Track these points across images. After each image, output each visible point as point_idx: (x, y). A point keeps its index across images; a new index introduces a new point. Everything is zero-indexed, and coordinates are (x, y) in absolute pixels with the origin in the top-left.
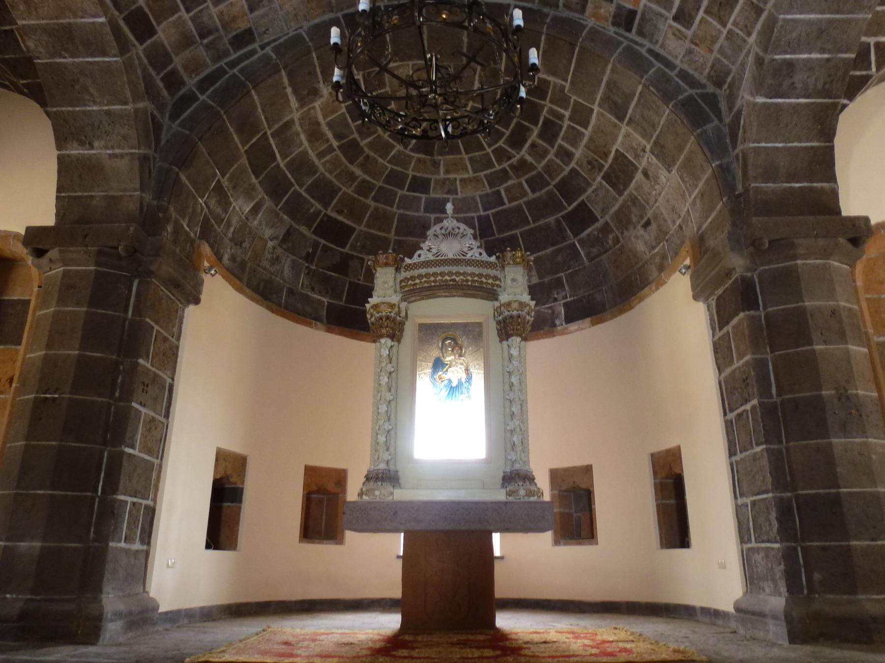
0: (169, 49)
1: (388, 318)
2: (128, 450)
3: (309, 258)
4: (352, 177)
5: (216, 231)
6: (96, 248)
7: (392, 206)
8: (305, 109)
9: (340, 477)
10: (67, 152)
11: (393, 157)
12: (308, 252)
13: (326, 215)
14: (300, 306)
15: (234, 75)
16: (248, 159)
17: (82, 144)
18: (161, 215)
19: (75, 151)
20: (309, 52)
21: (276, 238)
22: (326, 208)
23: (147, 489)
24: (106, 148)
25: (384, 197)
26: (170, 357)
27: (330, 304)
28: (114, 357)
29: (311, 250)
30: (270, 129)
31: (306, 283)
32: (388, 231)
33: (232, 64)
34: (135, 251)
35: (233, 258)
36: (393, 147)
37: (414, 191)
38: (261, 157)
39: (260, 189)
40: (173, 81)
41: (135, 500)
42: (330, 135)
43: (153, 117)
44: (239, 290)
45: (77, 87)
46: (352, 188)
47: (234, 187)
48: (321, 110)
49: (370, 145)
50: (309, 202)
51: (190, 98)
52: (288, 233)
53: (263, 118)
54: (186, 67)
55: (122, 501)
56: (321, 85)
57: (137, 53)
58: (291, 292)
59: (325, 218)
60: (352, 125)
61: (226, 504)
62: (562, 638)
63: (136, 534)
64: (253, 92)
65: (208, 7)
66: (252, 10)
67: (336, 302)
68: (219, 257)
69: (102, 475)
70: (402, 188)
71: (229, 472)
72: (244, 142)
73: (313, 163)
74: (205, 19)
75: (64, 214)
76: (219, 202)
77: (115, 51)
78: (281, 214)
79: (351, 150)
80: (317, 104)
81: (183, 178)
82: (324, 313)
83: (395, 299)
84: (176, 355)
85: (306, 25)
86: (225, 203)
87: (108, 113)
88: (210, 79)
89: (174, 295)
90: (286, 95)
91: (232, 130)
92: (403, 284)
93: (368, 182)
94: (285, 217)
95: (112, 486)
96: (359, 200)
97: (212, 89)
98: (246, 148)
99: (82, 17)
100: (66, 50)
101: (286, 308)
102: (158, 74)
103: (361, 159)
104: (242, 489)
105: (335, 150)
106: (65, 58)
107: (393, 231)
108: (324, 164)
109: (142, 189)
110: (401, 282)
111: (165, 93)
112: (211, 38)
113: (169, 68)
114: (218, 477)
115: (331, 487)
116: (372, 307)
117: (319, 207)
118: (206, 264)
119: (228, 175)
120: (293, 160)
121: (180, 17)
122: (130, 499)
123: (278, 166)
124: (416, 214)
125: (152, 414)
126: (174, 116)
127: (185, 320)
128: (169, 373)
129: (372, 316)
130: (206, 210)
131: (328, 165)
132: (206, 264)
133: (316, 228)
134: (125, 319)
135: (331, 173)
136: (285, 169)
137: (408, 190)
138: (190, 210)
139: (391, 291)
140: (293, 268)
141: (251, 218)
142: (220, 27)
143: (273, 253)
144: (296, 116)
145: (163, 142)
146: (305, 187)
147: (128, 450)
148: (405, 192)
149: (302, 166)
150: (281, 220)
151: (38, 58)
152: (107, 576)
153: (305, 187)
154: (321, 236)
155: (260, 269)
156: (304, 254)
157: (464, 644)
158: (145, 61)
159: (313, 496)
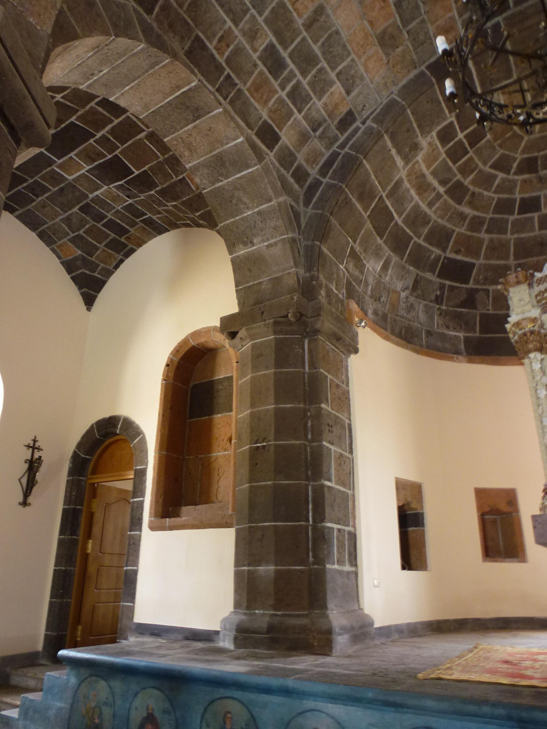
0: (292, 148)
1: (532, 332)
2: (327, 483)
3: (438, 300)
4: (462, 217)
5: (357, 291)
6: (272, 320)
7: (506, 233)
8: (410, 166)
9: (510, 497)
10: (237, 254)
11: (498, 186)
12: (437, 296)
13: (445, 258)
14: (439, 344)
15: (347, 153)
16: (371, 223)
17: (245, 244)
18: (314, 283)
19: (242, 251)
20: (404, 110)
21: (407, 288)
22: (444, 252)
23: (346, 516)
24: (264, 242)
25: (497, 227)
26: (344, 401)
27: (466, 338)
28: (302, 406)
29: (438, 293)
30: (384, 192)
31: (440, 322)
32: (507, 258)
33: (342, 146)
34: (302, 315)
35: (375, 313)
36: (496, 177)
37: (525, 213)
38: (381, 218)
39: (386, 248)
40: (300, 175)
41: (339, 527)
42: (435, 183)
43: (292, 207)
44: (386, 338)
45: (234, 201)
46: (465, 227)
47: (365, 251)
48: (424, 162)
49: (474, 182)
50: (429, 250)
51: (317, 184)
52: (416, 282)
53: (377, 183)
54: (307, 161)
55: (330, 528)
56: (420, 138)
57: (270, 160)
58: (429, 333)
59: (446, 261)
60: (454, 168)
61: (410, 529)
63: (345, 557)
64: (364, 161)
65: (314, 103)
66: (348, 93)
67: (470, 335)
68: (366, 314)
69: (310, 507)
70: (512, 213)
71: (409, 499)
72: (366, 209)
73: (426, 213)
74: (314, 114)
75: (244, 302)
76: (356, 266)
77: (255, 161)
78: (407, 266)
79: (457, 192)
80: (420, 157)
81: (325, 250)
82: (462, 346)
83: (535, 313)
84: (348, 399)
85: (395, 89)
86: (361, 267)
87: (259, 213)
88: (329, 163)
89: (337, 348)
90: (392, 156)
91: (354, 200)
92: (539, 298)
93: (479, 217)
94: (411, 268)
95: (320, 516)
96: (473, 237)
97: (331, 171)
98: (368, 213)
99: (227, 144)
100: (222, 175)
101: (428, 347)
102: (288, 172)
103: (467, 197)
104: (423, 514)
105: (442, 196)
106: (222, 181)
107: (512, 257)
108: (435, 212)
109: (296, 265)
110: (536, 296)
111: (296, 186)
112: (321, 129)
113: (295, 165)
114: (401, 504)
115: (503, 507)
116: (513, 325)
117: (438, 252)
118: (357, 319)
119: (358, 241)
120: (408, 216)
121: (295, 119)
122: (335, 526)
123: (396, 223)
124: (532, 234)
125: (339, 450)
126: (307, 203)
127: (349, 369)
128: (345, 414)
129: (514, 336)
130: (347, 274)
131: (439, 212)
132: (357, 319)
133: (439, 272)
134: (304, 373)
135: (443, 218)
136: (403, 225)
137: (519, 213)
138: (335, 276)
139: (529, 307)
140: (427, 312)
141: (383, 275)
142: (327, 117)
143: (406, 302)
144: (403, 174)
145: (303, 226)
146: (423, 237)
147: (327, 483)
148: (516, 216)
149: (417, 219)
150: (408, 272)
151: (204, 189)
152: (329, 595)
153: (423, 237)
154: (446, 279)
155: (398, 318)
156: (433, 297)
158: (277, 164)
159: (486, 517)
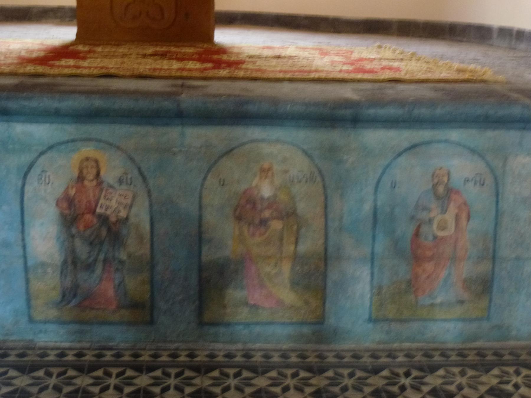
62: (306, 54)
157: (163, 55)
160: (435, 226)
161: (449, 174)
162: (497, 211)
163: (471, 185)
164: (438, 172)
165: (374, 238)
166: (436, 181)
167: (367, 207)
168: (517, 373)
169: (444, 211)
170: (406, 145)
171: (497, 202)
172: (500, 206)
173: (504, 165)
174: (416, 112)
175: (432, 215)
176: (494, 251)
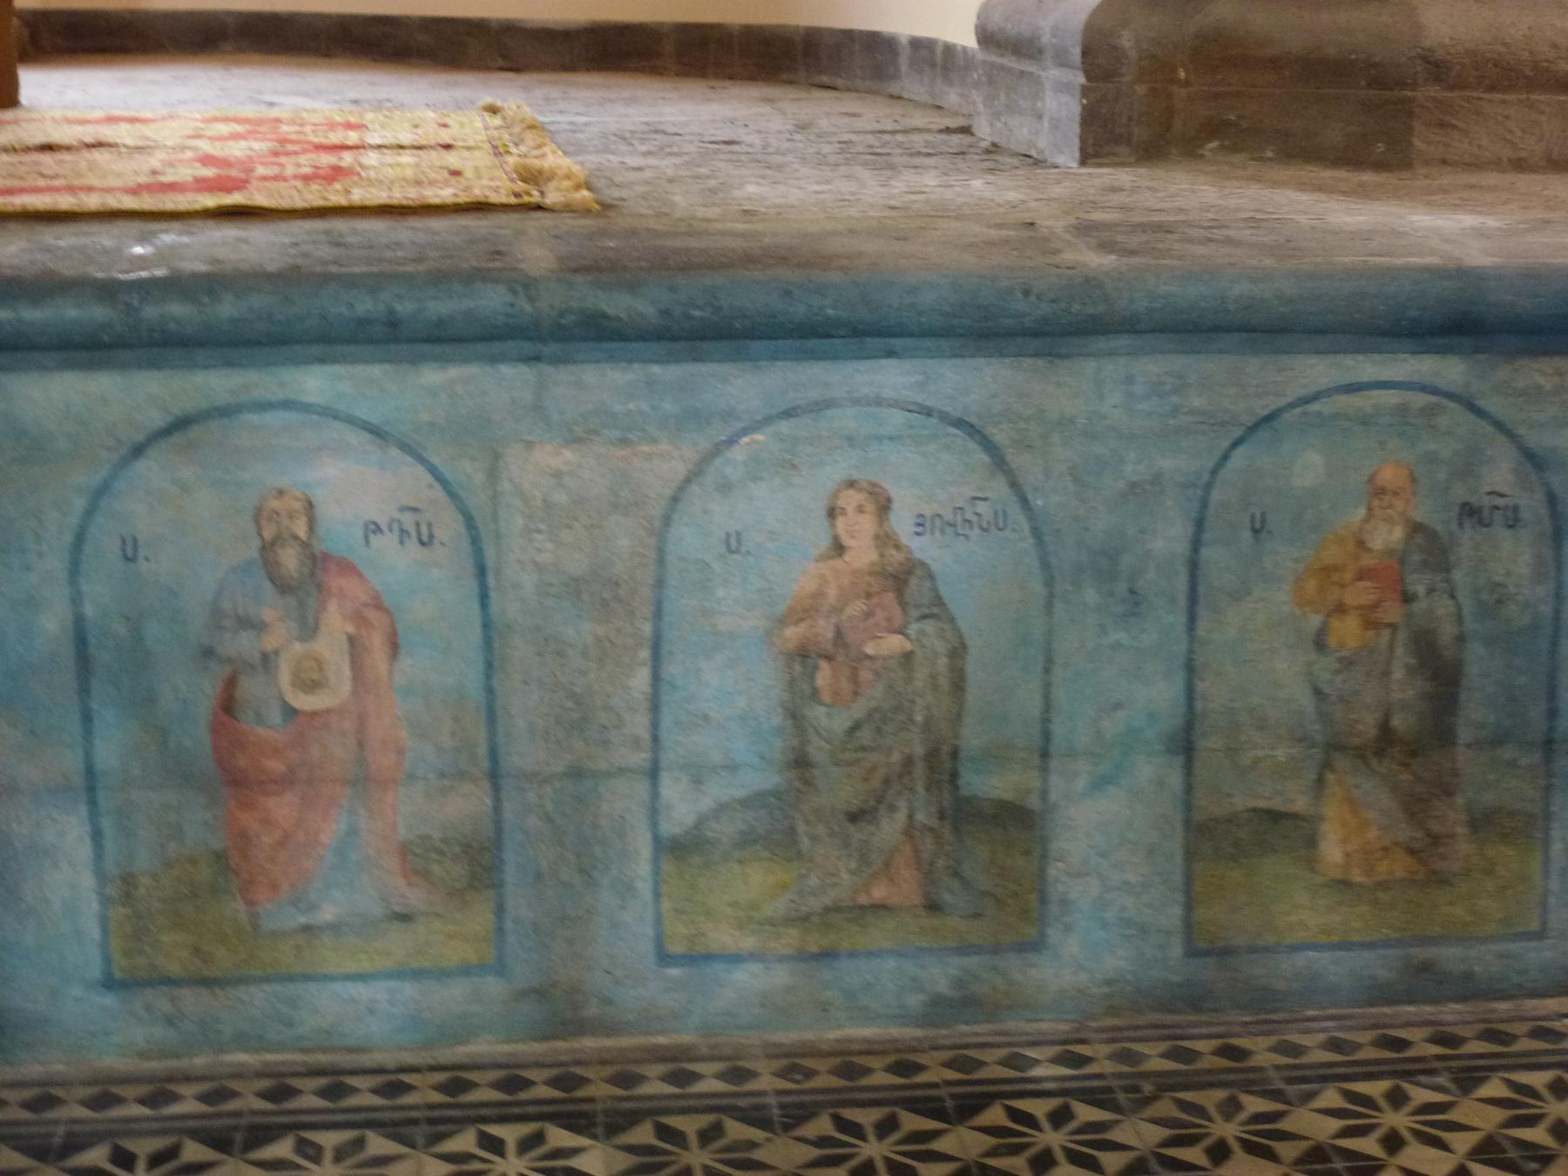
160: (285, 677)
161: (310, 506)
162: (487, 625)
163: (386, 542)
164: (275, 504)
165: (87, 718)
166: (267, 535)
167: (53, 623)
168: (1397, 1099)
169: (309, 630)
170: (157, 419)
171: (484, 598)
172: (494, 609)
173: (493, 474)
174: (151, 312)
175: (270, 642)
176: (493, 754)
